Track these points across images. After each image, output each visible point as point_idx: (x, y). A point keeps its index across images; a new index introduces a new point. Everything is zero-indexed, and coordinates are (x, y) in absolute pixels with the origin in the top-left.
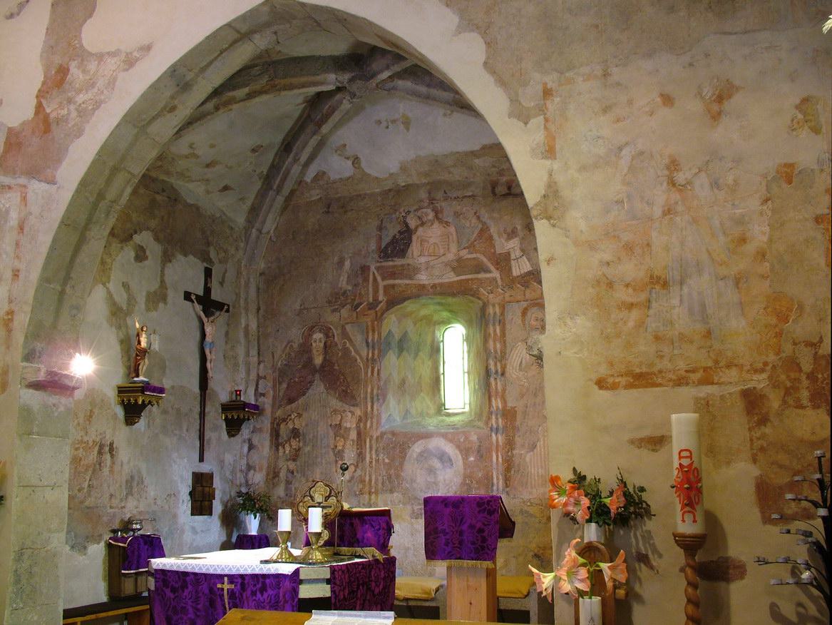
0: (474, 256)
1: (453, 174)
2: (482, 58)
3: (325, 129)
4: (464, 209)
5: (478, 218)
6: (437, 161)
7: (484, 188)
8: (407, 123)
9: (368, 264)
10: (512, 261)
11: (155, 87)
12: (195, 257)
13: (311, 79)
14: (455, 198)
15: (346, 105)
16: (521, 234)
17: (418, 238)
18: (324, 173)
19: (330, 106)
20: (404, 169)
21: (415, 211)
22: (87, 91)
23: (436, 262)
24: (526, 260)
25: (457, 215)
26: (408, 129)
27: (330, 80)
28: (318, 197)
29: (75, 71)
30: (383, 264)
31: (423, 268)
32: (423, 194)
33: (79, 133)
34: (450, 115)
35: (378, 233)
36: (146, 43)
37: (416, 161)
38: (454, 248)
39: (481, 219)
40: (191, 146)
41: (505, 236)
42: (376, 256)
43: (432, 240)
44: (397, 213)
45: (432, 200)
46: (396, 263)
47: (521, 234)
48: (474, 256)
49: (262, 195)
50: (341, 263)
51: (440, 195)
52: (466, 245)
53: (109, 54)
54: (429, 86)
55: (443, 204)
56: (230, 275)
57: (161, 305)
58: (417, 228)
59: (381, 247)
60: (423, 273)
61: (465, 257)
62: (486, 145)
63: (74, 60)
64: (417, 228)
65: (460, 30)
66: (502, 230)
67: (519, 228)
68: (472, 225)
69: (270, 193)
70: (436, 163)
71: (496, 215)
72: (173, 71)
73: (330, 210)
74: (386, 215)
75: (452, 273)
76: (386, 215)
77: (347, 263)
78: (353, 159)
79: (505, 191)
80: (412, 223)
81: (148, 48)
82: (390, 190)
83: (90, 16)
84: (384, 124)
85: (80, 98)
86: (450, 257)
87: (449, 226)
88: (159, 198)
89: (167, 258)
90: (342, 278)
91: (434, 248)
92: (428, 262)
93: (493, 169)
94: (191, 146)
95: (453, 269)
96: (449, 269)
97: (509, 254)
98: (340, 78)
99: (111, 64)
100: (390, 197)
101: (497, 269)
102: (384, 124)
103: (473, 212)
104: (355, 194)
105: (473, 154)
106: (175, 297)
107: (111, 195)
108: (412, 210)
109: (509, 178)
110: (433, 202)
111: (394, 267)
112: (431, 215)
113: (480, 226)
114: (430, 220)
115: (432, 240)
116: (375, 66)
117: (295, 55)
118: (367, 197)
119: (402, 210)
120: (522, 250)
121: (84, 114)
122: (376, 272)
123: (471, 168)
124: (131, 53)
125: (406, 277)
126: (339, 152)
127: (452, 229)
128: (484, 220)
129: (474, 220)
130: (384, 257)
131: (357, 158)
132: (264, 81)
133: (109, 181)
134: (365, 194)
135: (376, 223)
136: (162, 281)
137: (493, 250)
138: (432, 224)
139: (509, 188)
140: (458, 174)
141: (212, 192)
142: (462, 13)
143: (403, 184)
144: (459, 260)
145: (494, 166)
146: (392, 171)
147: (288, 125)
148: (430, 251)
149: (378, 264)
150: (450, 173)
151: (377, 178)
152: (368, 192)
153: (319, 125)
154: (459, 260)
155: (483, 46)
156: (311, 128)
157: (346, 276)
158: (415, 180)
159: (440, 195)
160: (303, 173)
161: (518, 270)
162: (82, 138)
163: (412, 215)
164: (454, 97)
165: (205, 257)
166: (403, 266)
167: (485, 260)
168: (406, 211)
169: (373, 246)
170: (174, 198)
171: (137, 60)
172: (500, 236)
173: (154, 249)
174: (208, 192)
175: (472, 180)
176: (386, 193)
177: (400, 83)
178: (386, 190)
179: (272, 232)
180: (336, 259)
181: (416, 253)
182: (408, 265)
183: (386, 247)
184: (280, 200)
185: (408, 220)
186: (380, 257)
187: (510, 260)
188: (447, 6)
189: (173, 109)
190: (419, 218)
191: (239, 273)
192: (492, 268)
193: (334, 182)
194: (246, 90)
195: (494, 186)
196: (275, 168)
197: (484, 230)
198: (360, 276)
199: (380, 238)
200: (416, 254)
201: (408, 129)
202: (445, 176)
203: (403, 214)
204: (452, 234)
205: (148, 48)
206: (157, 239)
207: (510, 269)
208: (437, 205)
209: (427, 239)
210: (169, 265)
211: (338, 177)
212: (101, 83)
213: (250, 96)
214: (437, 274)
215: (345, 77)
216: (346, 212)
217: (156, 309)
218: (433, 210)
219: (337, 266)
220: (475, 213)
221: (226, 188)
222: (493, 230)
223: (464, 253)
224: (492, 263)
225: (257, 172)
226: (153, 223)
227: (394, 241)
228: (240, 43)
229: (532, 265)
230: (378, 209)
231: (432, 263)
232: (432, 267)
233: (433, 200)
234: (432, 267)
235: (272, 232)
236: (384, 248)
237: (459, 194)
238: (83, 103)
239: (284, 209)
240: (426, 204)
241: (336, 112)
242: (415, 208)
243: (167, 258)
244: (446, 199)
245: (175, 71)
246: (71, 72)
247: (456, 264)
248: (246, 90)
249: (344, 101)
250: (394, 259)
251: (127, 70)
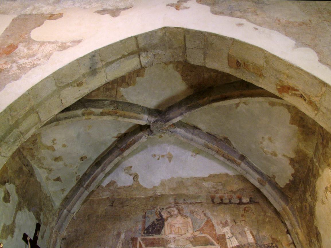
0: (203, 235)
1: (189, 190)
2: (317, 59)
3: (125, 154)
4: (196, 210)
5: (205, 214)
6: (182, 182)
7: (207, 199)
8: (170, 158)
9: (136, 237)
10: (227, 240)
11: (79, 61)
12: (33, 214)
13: (135, 115)
14: (190, 203)
15: (144, 139)
16: (230, 224)
17: (168, 224)
18: (114, 182)
19: (133, 140)
20: (163, 184)
21: (166, 209)
22: (28, 58)
23: (180, 238)
24: (235, 239)
25: (192, 212)
26: (170, 161)
27: (144, 119)
28: (107, 197)
29: (22, 49)
30: (146, 237)
31: (172, 240)
32: (171, 200)
33: (17, 78)
34: (195, 156)
35: (144, 219)
36: (78, 39)
37: (170, 180)
38: (191, 230)
39: (207, 215)
40: (54, 140)
41: (222, 225)
42: (142, 232)
43: (177, 226)
44: (156, 209)
45: (176, 204)
46: (155, 237)
47: (230, 224)
48: (203, 235)
49: (74, 190)
50: (119, 235)
51: (181, 201)
52: (198, 229)
53: (49, 42)
54: (193, 134)
55: (183, 206)
56: (47, 235)
57: (10, 237)
58: (167, 218)
59: (145, 227)
60: (172, 243)
61: (198, 236)
62: (212, 175)
63: (22, 43)
64: (167, 218)
65: (297, 46)
66: (219, 222)
67: (229, 221)
68: (201, 219)
69: (81, 189)
70: (181, 183)
71: (215, 213)
72: (93, 55)
73: (114, 205)
74: (148, 210)
75: (191, 245)
76: (148, 210)
77: (123, 236)
78: (134, 175)
79: (219, 201)
80: (165, 215)
81: (79, 42)
82: (151, 197)
83: (39, 26)
84: (157, 157)
85: (22, 61)
86: (189, 235)
87: (187, 218)
88: (24, 168)
89: (19, 207)
90: (118, 244)
91: (179, 229)
92: (175, 238)
93: (214, 189)
94: (54, 140)
95: (191, 242)
96: (188, 242)
97: (224, 235)
98: (149, 119)
99: (48, 48)
100: (151, 201)
101: (218, 243)
102: (157, 157)
103: (201, 211)
104: (129, 197)
105: (204, 179)
106: (18, 235)
107: (23, 127)
108: (165, 208)
109: (220, 195)
110: (178, 204)
111: (154, 239)
112: (176, 212)
113: (206, 219)
114: (175, 214)
115: (177, 226)
116: (171, 115)
117: (129, 101)
118: (137, 199)
119: (158, 207)
120: (232, 233)
121: (23, 69)
122: (141, 242)
123: (200, 188)
124: (65, 43)
125: (161, 246)
126: (126, 171)
127: (189, 220)
128: (208, 216)
129: (202, 216)
130: (146, 233)
131: (137, 175)
132: (111, 108)
133: (26, 116)
134: (136, 198)
135: (142, 214)
136: (14, 221)
137: (214, 233)
138: (177, 216)
139: (222, 200)
140: (192, 191)
141: (50, 180)
142: (296, 40)
143: (159, 194)
144: (195, 237)
145: (213, 188)
146: (155, 185)
147: (103, 149)
148: (176, 232)
149: (143, 237)
150: (187, 190)
151: (145, 188)
152: (138, 197)
153: (123, 151)
154: (195, 237)
155: (316, 54)
156: (117, 152)
157: (121, 243)
158: (167, 192)
159: (181, 201)
160: (102, 181)
161: (230, 244)
162: (17, 81)
163: (164, 211)
164: (205, 142)
165: (38, 217)
166: (159, 239)
167: (210, 238)
168: (161, 208)
169: (140, 226)
170: (32, 173)
171: (69, 47)
172: (218, 225)
173: (14, 197)
174: (47, 179)
175: (199, 195)
176: (148, 198)
177: (178, 130)
178: (148, 197)
179: (75, 214)
180: (115, 233)
181: (167, 232)
182: (163, 238)
183: (148, 228)
184: (86, 193)
185: (162, 213)
186: (144, 233)
187: (225, 239)
188: (286, 36)
189: (80, 84)
190: (169, 212)
191: (51, 235)
192: (215, 243)
193: (120, 188)
194: (101, 110)
195: (213, 198)
196: (86, 175)
197: (209, 221)
198: (131, 243)
199: (145, 222)
200: (167, 232)
201: (170, 161)
202: (185, 192)
203: (159, 210)
204: (189, 223)
205: (79, 42)
206: (17, 192)
207: (226, 244)
208: (179, 206)
209: (174, 224)
210: (19, 212)
211: (122, 185)
212: (39, 55)
213: (102, 114)
214: (181, 244)
215: (153, 119)
216: (123, 206)
217: (6, 238)
218: (177, 209)
219: (115, 237)
220: (203, 212)
221: (58, 179)
222: (214, 222)
223: (197, 234)
224: (215, 240)
225: (77, 175)
226: (18, 182)
227: (153, 225)
228: (133, 56)
229: (239, 242)
230: (144, 206)
231: (177, 238)
232: (178, 241)
233: (177, 203)
234: (178, 241)
235: (75, 214)
236: (147, 228)
237: (193, 201)
238: (24, 64)
239: (85, 201)
240: (173, 206)
241: (136, 144)
242: (167, 207)
243: (19, 207)
244: (185, 203)
245: (94, 56)
246: (18, 48)
247: (192, 239)
248: (101, 110)
249: (144, 137)
250: (153, 235)
251: (61, 51)
